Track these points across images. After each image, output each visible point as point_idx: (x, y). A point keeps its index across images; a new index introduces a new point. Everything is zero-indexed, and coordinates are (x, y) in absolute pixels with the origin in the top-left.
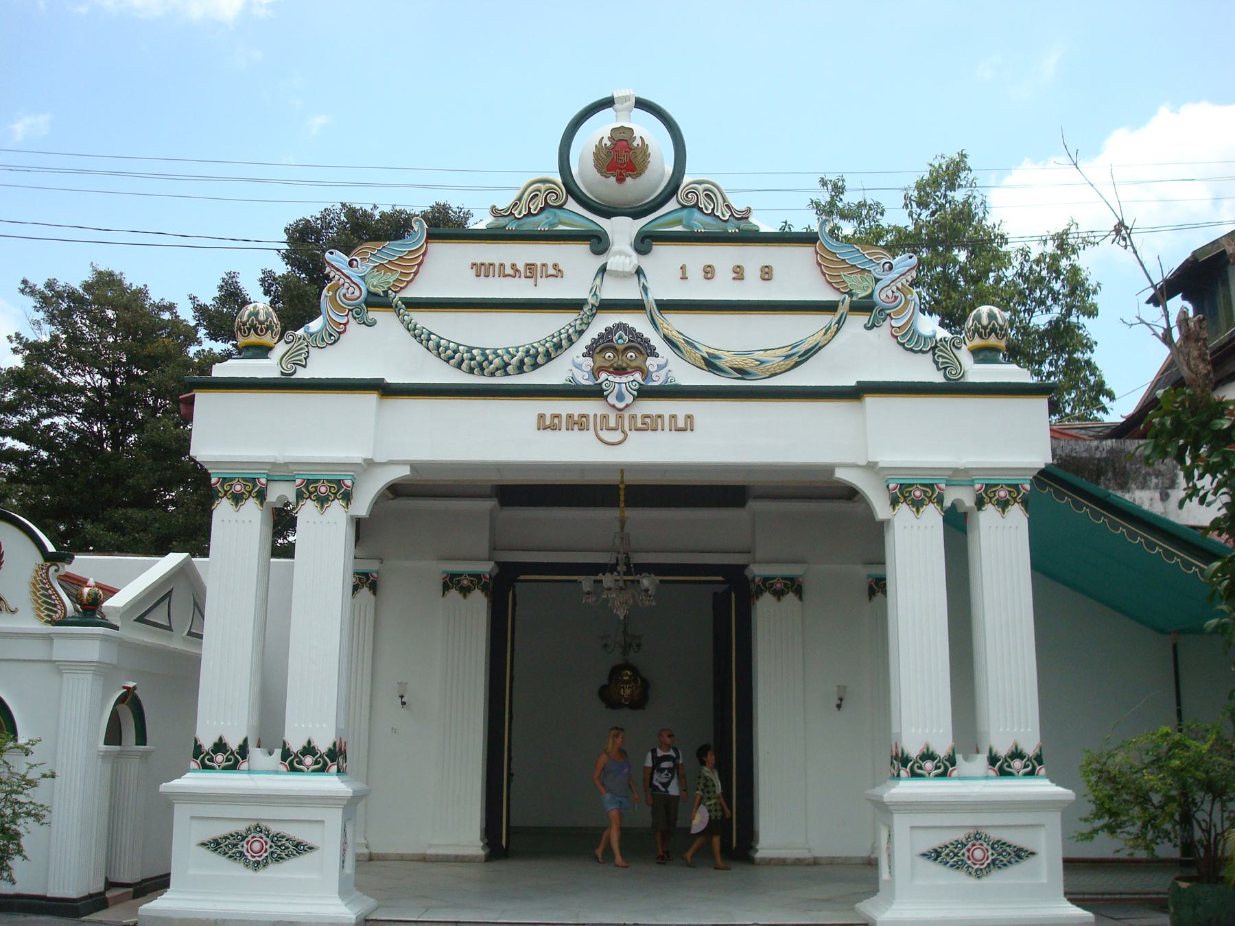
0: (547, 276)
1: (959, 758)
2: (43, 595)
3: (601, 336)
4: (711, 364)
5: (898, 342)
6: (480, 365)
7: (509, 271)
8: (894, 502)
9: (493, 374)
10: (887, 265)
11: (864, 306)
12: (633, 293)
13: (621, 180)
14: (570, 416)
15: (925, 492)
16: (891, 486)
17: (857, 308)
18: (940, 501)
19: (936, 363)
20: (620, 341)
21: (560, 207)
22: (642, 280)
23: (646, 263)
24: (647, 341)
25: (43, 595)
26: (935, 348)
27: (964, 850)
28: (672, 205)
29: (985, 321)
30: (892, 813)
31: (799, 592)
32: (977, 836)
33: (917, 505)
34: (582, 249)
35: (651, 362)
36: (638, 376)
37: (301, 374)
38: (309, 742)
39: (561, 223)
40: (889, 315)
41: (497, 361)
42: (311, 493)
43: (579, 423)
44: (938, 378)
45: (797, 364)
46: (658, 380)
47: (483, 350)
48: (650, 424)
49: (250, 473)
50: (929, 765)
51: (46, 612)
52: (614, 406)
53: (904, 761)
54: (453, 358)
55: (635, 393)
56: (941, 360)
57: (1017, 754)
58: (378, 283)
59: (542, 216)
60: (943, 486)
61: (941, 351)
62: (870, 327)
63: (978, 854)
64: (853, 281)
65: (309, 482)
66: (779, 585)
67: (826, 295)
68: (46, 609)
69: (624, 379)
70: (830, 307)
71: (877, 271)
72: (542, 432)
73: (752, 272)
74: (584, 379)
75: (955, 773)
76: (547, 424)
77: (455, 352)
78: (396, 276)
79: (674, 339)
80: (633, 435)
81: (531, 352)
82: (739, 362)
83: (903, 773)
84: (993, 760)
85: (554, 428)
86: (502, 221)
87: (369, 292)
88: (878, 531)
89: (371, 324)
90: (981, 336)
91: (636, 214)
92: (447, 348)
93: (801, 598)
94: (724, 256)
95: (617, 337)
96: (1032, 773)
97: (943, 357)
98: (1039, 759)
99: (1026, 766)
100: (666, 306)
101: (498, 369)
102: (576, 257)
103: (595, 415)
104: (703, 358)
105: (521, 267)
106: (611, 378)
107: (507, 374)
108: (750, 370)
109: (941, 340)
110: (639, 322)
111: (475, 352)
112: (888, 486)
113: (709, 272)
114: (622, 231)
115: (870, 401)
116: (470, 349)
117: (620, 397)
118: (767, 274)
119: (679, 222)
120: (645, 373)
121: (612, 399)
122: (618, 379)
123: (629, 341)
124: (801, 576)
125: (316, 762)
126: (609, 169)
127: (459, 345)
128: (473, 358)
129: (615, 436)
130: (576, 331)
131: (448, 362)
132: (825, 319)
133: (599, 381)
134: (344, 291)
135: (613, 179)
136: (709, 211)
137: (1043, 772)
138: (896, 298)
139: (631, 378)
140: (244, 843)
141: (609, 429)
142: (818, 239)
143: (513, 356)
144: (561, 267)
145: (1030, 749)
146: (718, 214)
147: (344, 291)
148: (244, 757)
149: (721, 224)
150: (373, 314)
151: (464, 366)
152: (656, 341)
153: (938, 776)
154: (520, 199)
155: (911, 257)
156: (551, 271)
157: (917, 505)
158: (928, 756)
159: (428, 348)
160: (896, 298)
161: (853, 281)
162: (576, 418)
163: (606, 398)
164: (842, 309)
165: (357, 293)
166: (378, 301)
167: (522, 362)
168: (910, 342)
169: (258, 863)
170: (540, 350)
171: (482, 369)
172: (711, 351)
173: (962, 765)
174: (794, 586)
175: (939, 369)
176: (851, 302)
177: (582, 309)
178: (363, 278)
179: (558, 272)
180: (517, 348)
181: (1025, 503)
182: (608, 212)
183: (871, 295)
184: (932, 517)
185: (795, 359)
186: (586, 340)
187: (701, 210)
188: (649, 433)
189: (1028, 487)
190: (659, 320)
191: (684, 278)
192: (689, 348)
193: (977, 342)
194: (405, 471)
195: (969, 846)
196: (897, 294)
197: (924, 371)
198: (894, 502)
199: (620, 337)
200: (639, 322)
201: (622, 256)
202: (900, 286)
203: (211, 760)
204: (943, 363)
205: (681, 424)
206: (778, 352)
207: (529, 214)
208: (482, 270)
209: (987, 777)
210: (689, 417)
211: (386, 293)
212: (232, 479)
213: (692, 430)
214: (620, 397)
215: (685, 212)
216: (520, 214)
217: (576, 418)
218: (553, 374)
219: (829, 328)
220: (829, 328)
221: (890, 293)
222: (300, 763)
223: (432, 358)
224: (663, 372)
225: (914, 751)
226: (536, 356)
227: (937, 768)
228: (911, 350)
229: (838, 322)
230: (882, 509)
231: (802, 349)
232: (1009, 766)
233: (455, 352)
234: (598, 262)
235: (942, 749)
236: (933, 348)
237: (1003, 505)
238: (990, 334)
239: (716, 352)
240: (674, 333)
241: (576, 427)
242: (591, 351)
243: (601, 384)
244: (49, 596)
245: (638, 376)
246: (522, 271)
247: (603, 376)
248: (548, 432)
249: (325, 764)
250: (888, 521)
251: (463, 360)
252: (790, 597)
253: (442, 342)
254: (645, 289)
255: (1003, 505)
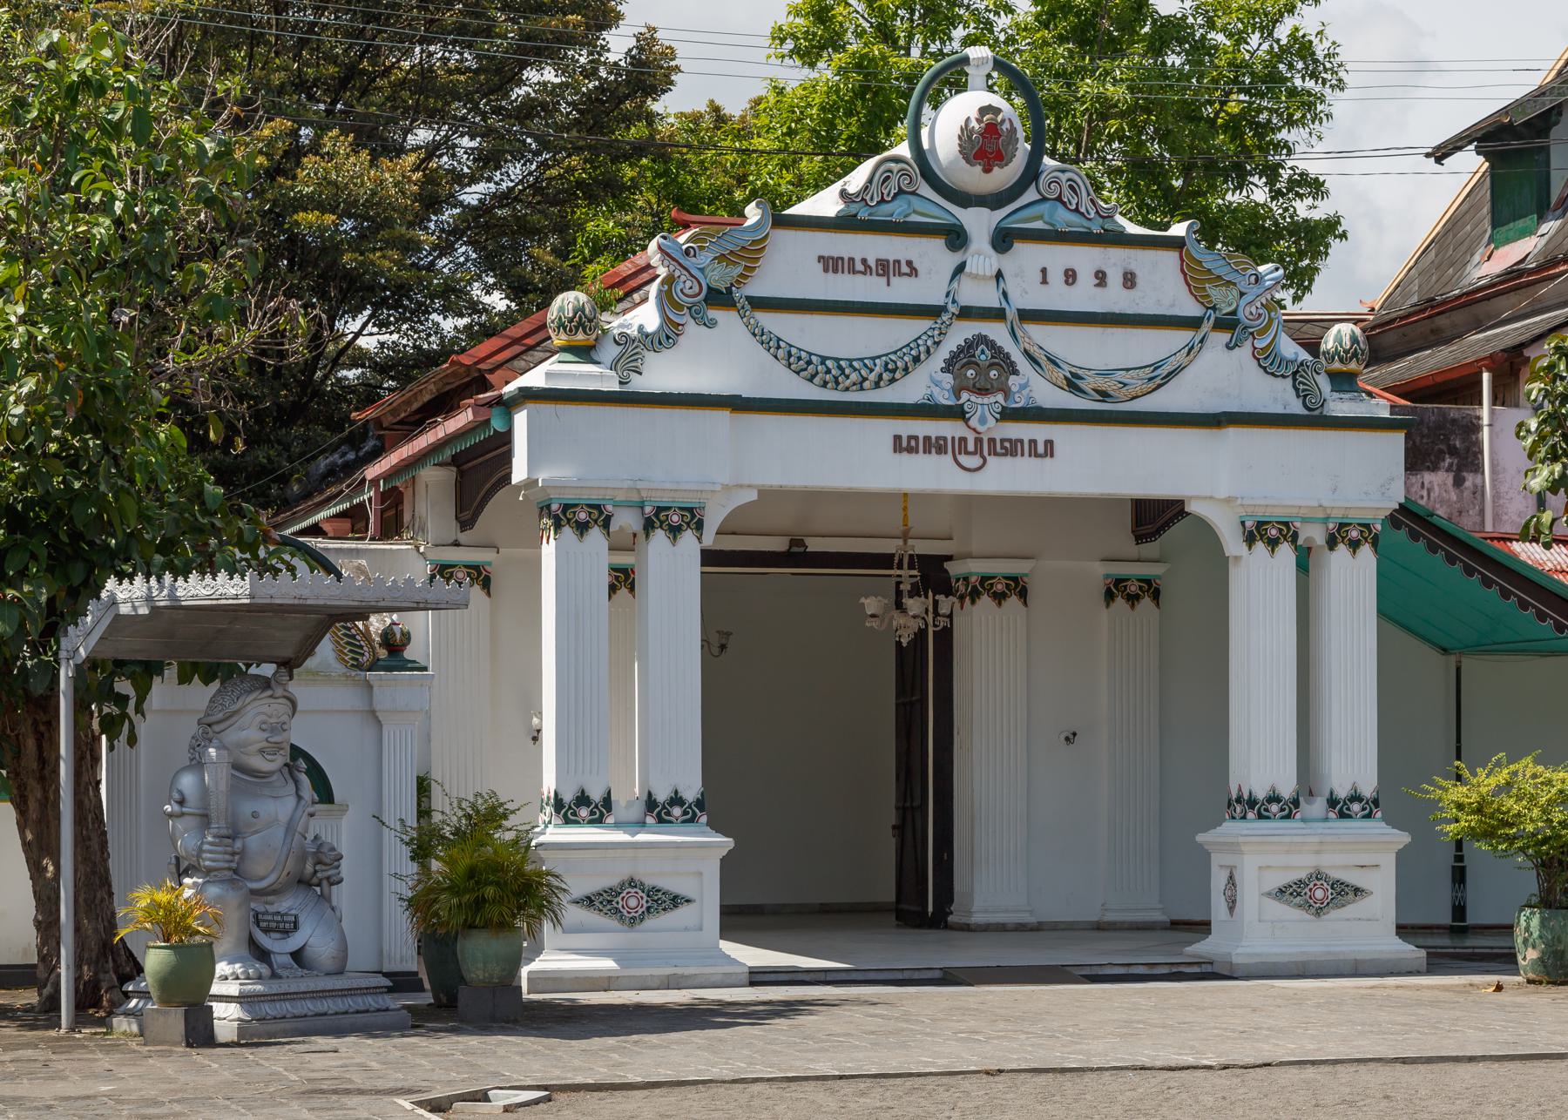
0: (901, 274)
1: (1301, 799)
2: (345, 635)
3: (961, 350)
4: (1073, 384)
5: (1260, 365)
6: (836, 378)
7: (860, 267)
8: (1250, 539)
9: (847, 389)
10: (1253, 278)
11: (1227, 324)
12: (991, 299)
13: (987, 170)
14: (927, 439)
15: (1280, 530)
16: (1249, 524)
17: (1221, 325)
18: (1295, 536)
19: (1297, 390)
20: (983, 357)
21: (913, 193)
22: (1002, 284)
23: (1008, 262)
24: (1008, 356)
25: (345, 635)
26: (1297, 374)
27: (1307, 890)
28: (1031, 195)
29: (1347, 343)
30: (1242, 853)
31: (1023, 594)
32: (1318, 876)
33: (1273, 544)
34: (936, 245)
35: (1013, 381)
36: (1000, 397)
37: (639, 384)
38: (676, 792)
39: (915, 212)
40: (1252, 334)
41: (854, 377)
42: (662, 523)
43: (936, 446)
44: (1296, 407)
45: (1159, 386)
46: (1020, 402)
47: (837, 360)
48: (1011, 448)
49: (594, 498)
50: (1274, 808)
51: (351, 655)
52: (974, 430)
53: (1252, 803)
54: (806, 369)
55: (998, 416)
56: (1301, 387)
57: (1356, 798)
58: (719, 276)
59: (896, 203)
60: (1298, 524)
61: (1302, 376)
62: (1229, 347)
63: (1319, 894)
64: (1216, 294)
65: (659, 510)
66: (1000, 587)
67: (1191, 309)
68: (351, 651)
69: (986, 400)
70: (1193, 323)
71: (1243, 286)
72: (897, 455)
73: (1114, 278)
74: (945, 399)
75: (1298, 816)
76: (902, 446)
77: (809, 363)
78: (739, 270)
79: (1036, 355)
80: (991, 460)
81: (890, 366)
82: (1102, 383)
83: (1251, 815)
84: (1332, 802)
85: (911, 450)
86: (853, 209)
87: (709, 288)
88: (1219, 565)
89: (711, 324)
90: (1341, 360)
91: (994, 201)
92: (799, 359)
93: (1025, 603)
94: (1085, 258)
95: (978, 352)
96: (1369, 816)
97: (1304, 384)
98: (1376, 802)
99: (1364, 809)
100: (1027, 316)
101: (854, 384)
102: (931, 255)
103: (953, 438)
104: (1066, 378)
105: (872, 263)
106: (973, 398)
107: (862, 389)
108: (1112, 393)
109: (1302, 364)
110: (997, 332)
111: (829, 363)
112: (1243, 523)
113: (1070, 276)
114: (979, 223)
115: (1232, 433)
116: (823, 359)
117: (983, 421)
118: (1129, 280)
119: (1040, 217)
120: (1007, 393)
121: (974, 422)
122: (979, 400)
123: (993, 357)
124: (1027, 575)
125: (685, 813)
126: (976, 157)
127: (810, 354)
128: (828, 371)
129: (973, 461)
130: (935, 343)
131: (798, 373)
132: (1183, 337)
133: (961, 401)
134: (681, 286)
135: (978, 169)
136: (1074, 207)
137: (1379, 815)
138: (1260, 315)
139: (992, 399)
140: (619, 899)
141: (967, 453)
142: (1184, 244)
143: (872, 371)
144: (915, 264)
145: (1368, 790)
146: (1083, 210)
147: (681, 286)
148: (609, 809)
149: (1086, 223)
150: (713, 313)
151: (817, 380)
152: (1017, 357)
153: (1282, 818)
154: (870, 181)
155: (1277, 269)
156: (905, 269)
157: (1273, 544)
158: (1274, 798)
159: (776, 357)
160: (1260, 315)
161: (1216, 294)
162: (933, 440)
163: (966, 421)
164: (1206, 326)
165: (696, 289)
166: (719, 298)
167: (880, 377)
168: (1269, 361)
169: (634, 918)
170: (899, 364)
171: (837, 383)
172: (1073, 370)
173: (1306, 808)
174: (1018, 587)
175: (1298, 396)
176: (1216, 318)
177: (939, 316)
178: (702, 270)
179: (913, 272)
180: (873, 359)
181: (1375, 543)
182: (964, 199)
183: (1234, 313)
184: (1286, 552)
185: (1158, 381)
186: (943, 353)
187: (1064, 204)
188: (1009, 459)
189: (1379, 527)
190: (1019, 333)
191: (1044, 281)
192: (1051, 366)
193: (1337, 365)
194: (753, 496)
195: (1311, 885)
196: (1261, 311)
197: (1278, 396)
198: (1250, 539)
199: (983, 352)
200: (997, 332)
201: (980, 256)
202: (1264, 302)
203: (574, 814)
204: (1304, 390)
205: (1041, 449)
206: (1141, 372)
207: (883, 201)
208: (831, 264)
209: (1326, 819)
210: (1049, 444)
211: (729, 290)
212: (576, 505)
213: (1052, 456)
214: (983, 421)
215: (1046, 206)
216: (872, 199)
217: (933, 440)
218: (911, 390)
219: (1192, 347)
220: (1192, 347)
221: (1253, 310)
222: (668, 814)
223: (779, 369)
224: (1025, 392)
225: (1261, 795)
226: (894, 371)
227: (1282, 810)
228: (1272, 374)
229: (1202, 341)
230: (1233, 544)
231: (1163, 371)
232: (1348, 809)
233: (809, 363)
234: (951, 260)
235: (1287, 790)
236: (1295, 374)
237: (1354, 545)
238: (1351, 359)
239: (1080, 372)
240: (1036, 348)
241: (933, 450)
242: (949, 366)
243: (962, 405)
244: (353, 637)
245: (1000, 397)
246: (873, 265)
247: (965, 396)
248: (905, 454)
249: (694, 814)
250: (1237, 559)
251: (817, 373)
252: (1013, 601)
253: (794, 351)
254: (1005, 294)
255: (1354, 545)
